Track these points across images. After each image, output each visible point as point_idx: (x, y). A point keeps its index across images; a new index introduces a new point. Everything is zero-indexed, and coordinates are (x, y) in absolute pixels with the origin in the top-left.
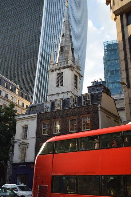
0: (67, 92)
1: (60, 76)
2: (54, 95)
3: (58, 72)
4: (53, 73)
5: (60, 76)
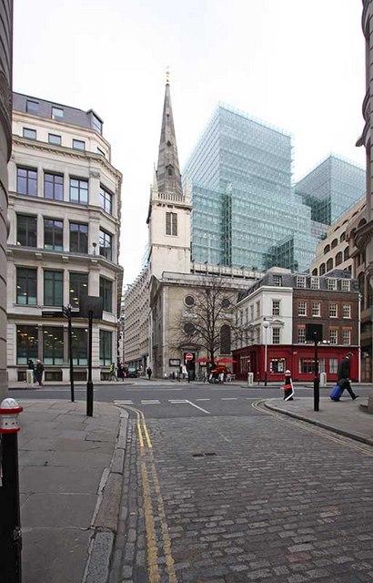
2: (164, 246)
3: (169, 210)
4: (159, 208)
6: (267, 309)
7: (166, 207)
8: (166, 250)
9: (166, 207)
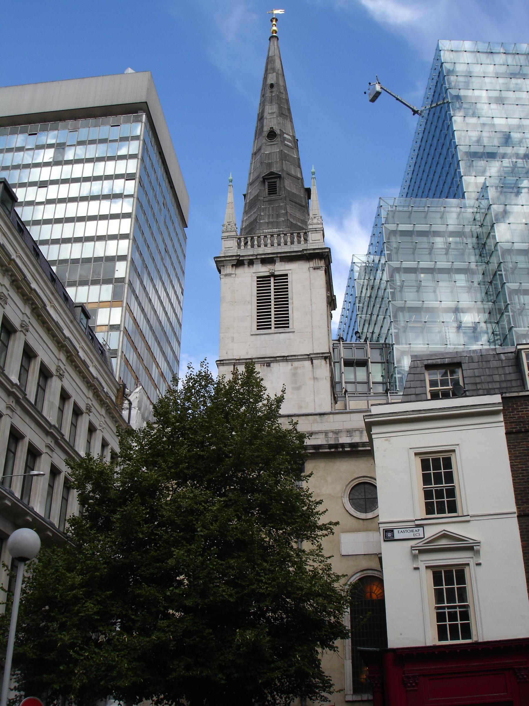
0: (310, 358)
1: (272, 288)
3: (263, 270)
4: (240, 271)
5: (272, 288)
6: (400, 491)
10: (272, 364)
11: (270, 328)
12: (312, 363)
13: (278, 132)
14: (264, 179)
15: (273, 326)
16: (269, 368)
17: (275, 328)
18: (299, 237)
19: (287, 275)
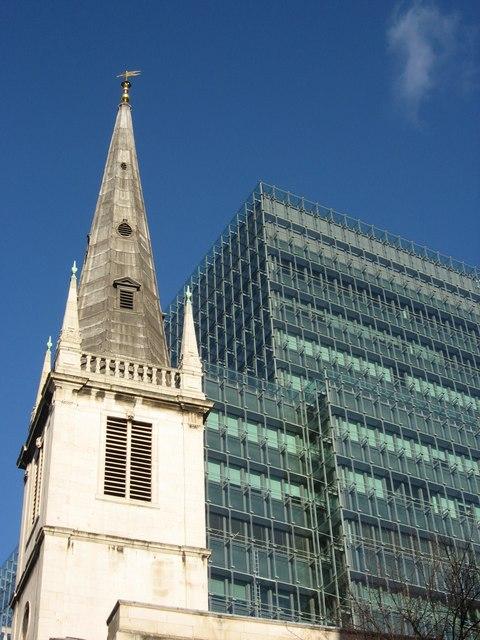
2: (93, 536)
3: (121, 410)
4: (83, 400)
7: (110, 398)
8: (101, 552)
9: (110, 398)
10: (125, 549)
11: (123, 496)
12: (184, 560)
13: (134, 228)
14: (115, 285)
15: (128, 493)
16: (121, 554)
17: (131, 497)
18: (159, 375)
19: (150, 425)
